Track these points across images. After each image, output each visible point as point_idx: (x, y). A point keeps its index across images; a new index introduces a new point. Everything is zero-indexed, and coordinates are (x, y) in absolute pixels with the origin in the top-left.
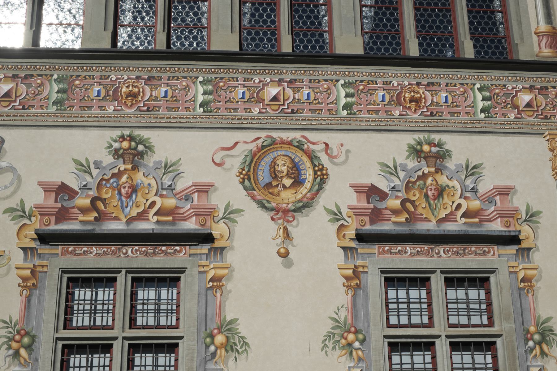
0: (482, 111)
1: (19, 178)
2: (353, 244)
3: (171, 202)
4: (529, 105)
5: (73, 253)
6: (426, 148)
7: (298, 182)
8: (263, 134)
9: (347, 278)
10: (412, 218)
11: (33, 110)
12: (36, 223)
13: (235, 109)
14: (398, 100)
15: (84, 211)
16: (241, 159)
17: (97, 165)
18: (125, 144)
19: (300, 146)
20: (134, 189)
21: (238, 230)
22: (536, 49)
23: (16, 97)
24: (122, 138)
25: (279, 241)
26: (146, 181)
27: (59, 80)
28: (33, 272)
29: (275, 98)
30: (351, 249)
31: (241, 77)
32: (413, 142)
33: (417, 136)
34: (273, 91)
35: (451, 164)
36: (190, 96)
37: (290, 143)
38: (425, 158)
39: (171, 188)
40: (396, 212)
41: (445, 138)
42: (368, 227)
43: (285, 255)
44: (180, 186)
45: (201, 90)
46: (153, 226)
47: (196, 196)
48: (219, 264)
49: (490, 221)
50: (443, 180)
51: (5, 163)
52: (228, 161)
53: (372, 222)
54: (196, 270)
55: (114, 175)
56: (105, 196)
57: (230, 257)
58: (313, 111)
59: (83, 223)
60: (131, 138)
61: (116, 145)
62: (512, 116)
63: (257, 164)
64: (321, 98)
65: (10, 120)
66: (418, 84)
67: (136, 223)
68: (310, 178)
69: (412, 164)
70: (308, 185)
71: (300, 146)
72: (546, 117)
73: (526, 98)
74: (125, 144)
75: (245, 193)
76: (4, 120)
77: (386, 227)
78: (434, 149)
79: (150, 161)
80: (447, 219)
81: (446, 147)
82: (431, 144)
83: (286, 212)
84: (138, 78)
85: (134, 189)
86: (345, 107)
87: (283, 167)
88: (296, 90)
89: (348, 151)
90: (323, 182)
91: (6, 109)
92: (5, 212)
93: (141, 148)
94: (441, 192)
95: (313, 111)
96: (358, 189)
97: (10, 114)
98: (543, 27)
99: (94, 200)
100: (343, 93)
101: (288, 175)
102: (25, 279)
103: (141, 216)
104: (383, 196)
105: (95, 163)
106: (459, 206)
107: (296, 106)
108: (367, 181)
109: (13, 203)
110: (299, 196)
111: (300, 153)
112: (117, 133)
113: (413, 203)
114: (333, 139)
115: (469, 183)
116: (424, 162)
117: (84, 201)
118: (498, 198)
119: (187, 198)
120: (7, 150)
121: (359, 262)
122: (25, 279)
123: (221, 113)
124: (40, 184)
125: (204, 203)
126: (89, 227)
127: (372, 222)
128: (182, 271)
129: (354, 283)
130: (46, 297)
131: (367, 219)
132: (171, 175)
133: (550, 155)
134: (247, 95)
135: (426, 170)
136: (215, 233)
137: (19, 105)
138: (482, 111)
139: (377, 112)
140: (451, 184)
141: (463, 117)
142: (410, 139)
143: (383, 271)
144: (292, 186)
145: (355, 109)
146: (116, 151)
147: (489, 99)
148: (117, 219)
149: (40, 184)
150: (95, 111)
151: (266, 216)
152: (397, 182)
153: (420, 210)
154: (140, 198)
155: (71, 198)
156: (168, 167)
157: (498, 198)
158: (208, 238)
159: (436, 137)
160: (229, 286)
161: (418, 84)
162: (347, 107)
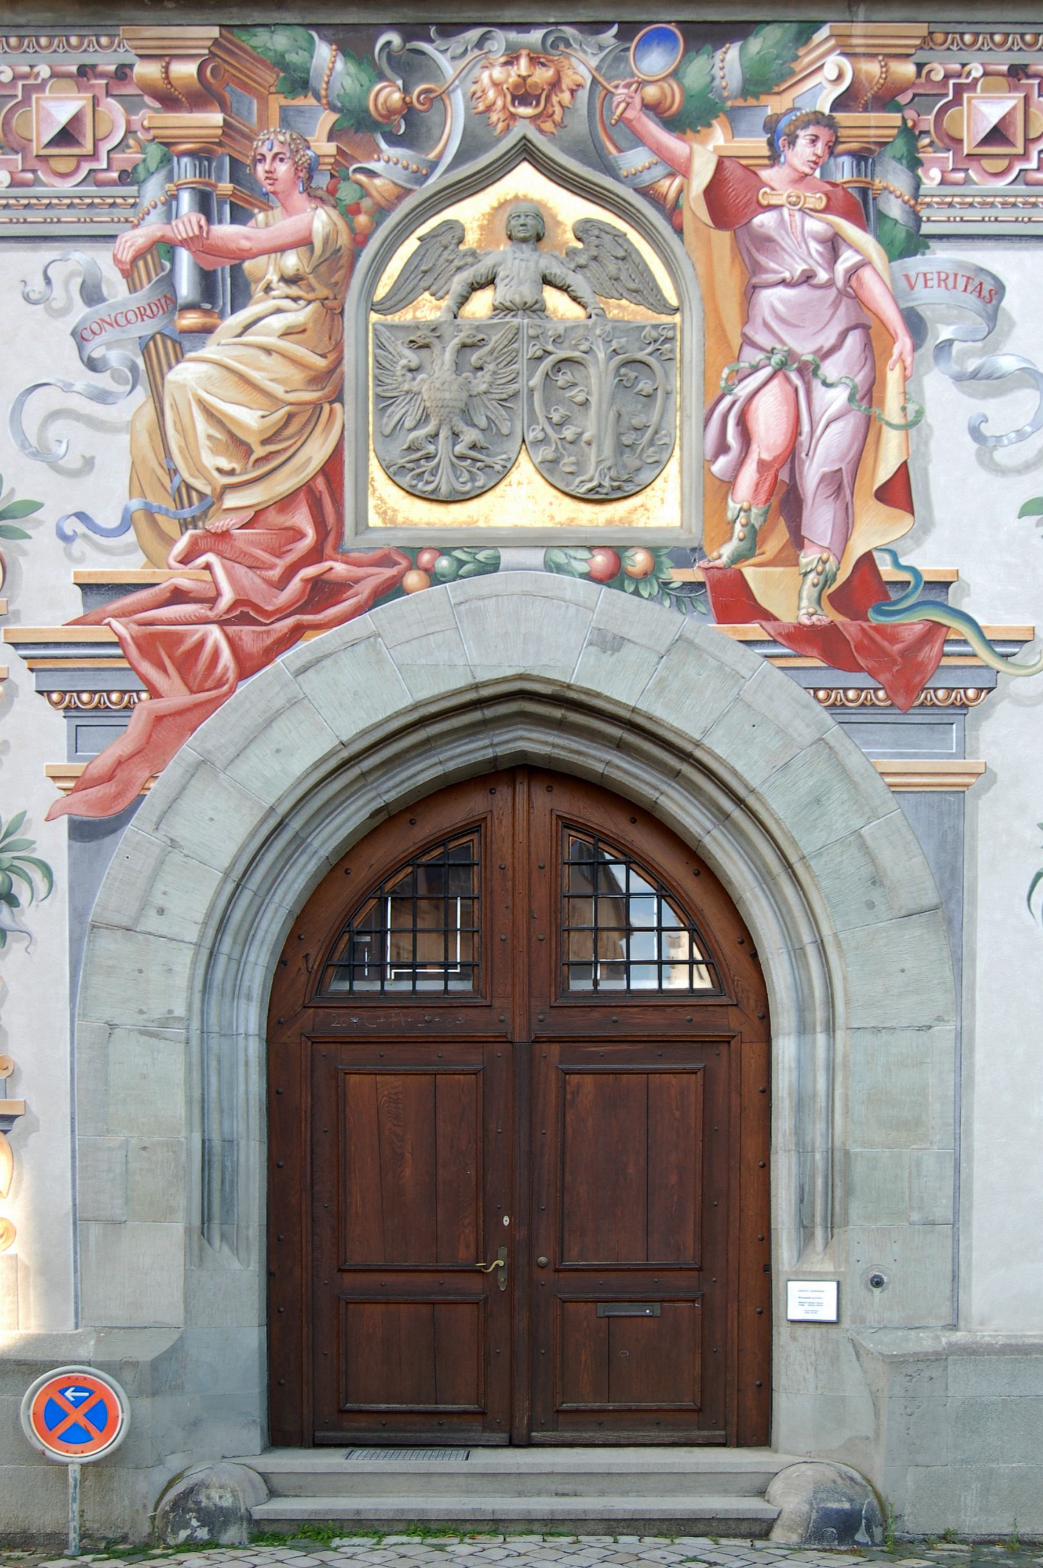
23: (1028, 141)
51: (1013, 358)
65: (1016, 221)
76: (996, 220)
91: (1001, 184)
97: (1012, 200)
120: (1015, 316)
137: (1038, 169)
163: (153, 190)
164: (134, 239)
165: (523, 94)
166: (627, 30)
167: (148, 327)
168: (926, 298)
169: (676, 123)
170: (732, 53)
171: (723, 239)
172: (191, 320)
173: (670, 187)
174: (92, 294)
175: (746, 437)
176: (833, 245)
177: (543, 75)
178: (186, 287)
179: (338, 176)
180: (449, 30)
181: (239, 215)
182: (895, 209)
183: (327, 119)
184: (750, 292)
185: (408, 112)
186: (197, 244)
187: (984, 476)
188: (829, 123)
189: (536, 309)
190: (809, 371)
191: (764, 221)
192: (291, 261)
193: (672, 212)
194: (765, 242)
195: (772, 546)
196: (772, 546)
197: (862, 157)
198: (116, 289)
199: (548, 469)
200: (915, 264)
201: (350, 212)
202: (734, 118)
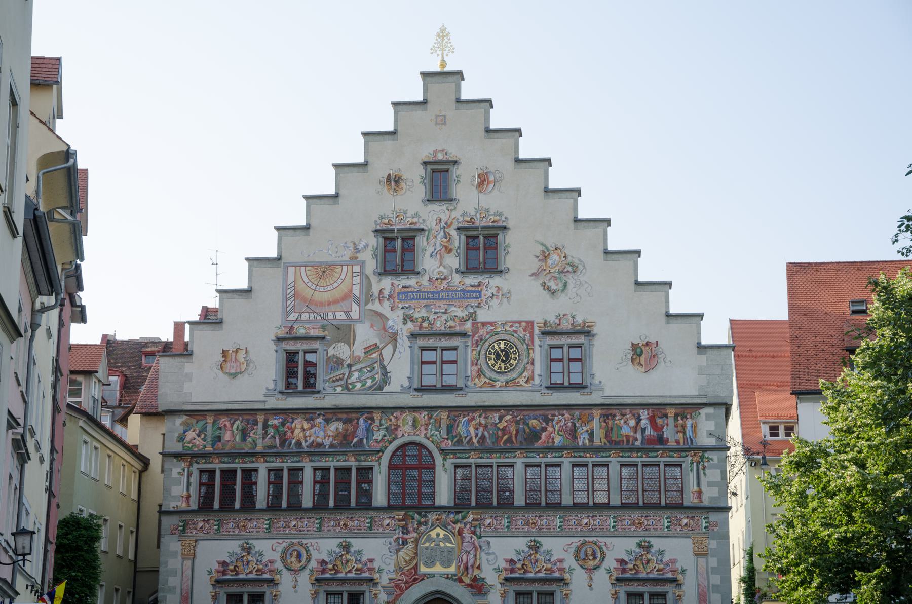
0: (667, 528)
1: (496, 557)
2: (615, 582)
3: (549, 566)
4: (686, 525)
5: (517, 584)
6: (643, 544)
7: (595, 558)
8: (582, 539)
9: (613, 595)
10: (637, 572)
11: (499, 530)
12: (503, 575)
13: (572, 529)
14: (633, 524)
15: (519, 569)
16: (574, 549)
17: (523, 551)
18: (532, 543)
19: (595, 544)
20: (537, 561)
21: (573, 576)
22: (691, 499)
24: (531, 540)
25: (588, 580)
26: (541, 558)
27: (507, 518)
28: (504, 592)
29: (586, 524)
30: (614, 584)
31: (573, 515)
32: (638, 541)
33: (640, 539)
34: (585, 521)
35: (653, 550)
36: (555, 524)
37: (592, 542)
38: (643, 548)
39: (549, 560)
40: (631, 569)
41: (651, 539)
42: (620, 576)
43: (590, 586)
44: (552, 560)
45: (559, 521)
46: (544, 575)
47: (558, 563)
48: (567, 589)
49: (667, 573)
50: (649, 556)
52: (569, 549)
53: (622, 574)
54: (559, 591)
55: (529, 555)
56: (526, 563)
57: (571, 586)
58: (600, 529)
59: (520, 574)
60: (535, 541)
61: (529, 544)
62: (679, 530)
63: (580, 551)
64: (604, 523)
66: (642, 516)
67: (538, 574)
68: (599, 556)
69: (638, 550)
70: (598, 559)
71: (595, 544)
72: (693, 530)
73: (685, 521)
74: (532, 543)
75: (575, 562)
77: (627, 575)
78: (647, 544)
79: (542, 550)
80: (650, 572)
81: (651, 543)
82: (645, 542)
83: (590, 569)
84: (536, 516)
85: (537, 561)
86: (613, 527)
87: (589, 552)
88: (594, 520)
89: (613, 545)
90: (604, 558)
92: (493, 569)
93: (538, 545)
94: (648, 561)
95: (600, 529)
96: (617, 560)
98: (696, 489)
99: (523, 565)
100: (612, 521)
101: (591, 555)
102: (502, 594)
103: (539, 571)
104: (626, 563)
105: (522, 551)
106: (655, 567)
107: (594, 527)
108: (620, 557)
109: (496, 566)
110: (595, 563)
111: (595, 546)
112: (529, 539)
113: (637, 566)
114: (608, 540)
115: (659, 558)
116: (642, 549)
117: (519, 566)
118: (670, 564)
119: (555, 564)
121: (617, 589)
122: (502, 594)
123: (566, 530)
124: (504, 559)
125: (561, 566)
126: (522, 576)
127: (622, 574)
128: (555, 591)
129: (615, 597)
130: (509, 600)
131: (620, 572)
132: (549, 555)
133: (693, 546)
134: (576, 523)
135: (643, 553)
136: (566, 577)
138: (667, 528)
139: (625, 529)
140: (652, 558)
141: (659, 530)
142: (637, 540)
143: (626, 592)
144: (593, 559)
145: (617, 528)
146: (529, 546)
147: (670, 522)
148: (531, 572)
149: (504, 559)
150: (521, 530)
151: (583, 571)
152: (632, 558)
153: (640, 569)
154: (538, 564)
155: (515, 564)
156: (548, 552)
157: (670, 564)
158: (562, 580)
159: (647, 539)
160: (571, 597)
161: (642, 516)
162: (614, 527)
163: (397, 531)
164: (395, 537)
165: (438, 520)
166: (449, 512)
167: (397, 547)
168: (482, 544)
169: (454, 523)
170: (460, 515)
171: (459, 537)
172: (401, 547)
173: (454, 531)
174: (390, 544)
175: (462, 561)
176: (471, 537)
177: (440, 517)
178: (401, 543)
179: (417, 529)
180: (429, 512)
181: (407, 534)
182: (478, 533)
183: (416, 523)
184: (462, 543)
185: (425, 522)
186: (402, 537)
187: (488, 566)
188: (471, 523)
189: (439, 545)
190: (469, 553)
191: (464, 535)
192: (412, 540)
193: (454, 533)
194: (464, 537)
195: (465, 574)
196: (465, 574)
197: (474, 527)
198: (393, 543)
199: (440, 564)
200: (480, 540)
201: (418, 534)
202: (460, 522)
